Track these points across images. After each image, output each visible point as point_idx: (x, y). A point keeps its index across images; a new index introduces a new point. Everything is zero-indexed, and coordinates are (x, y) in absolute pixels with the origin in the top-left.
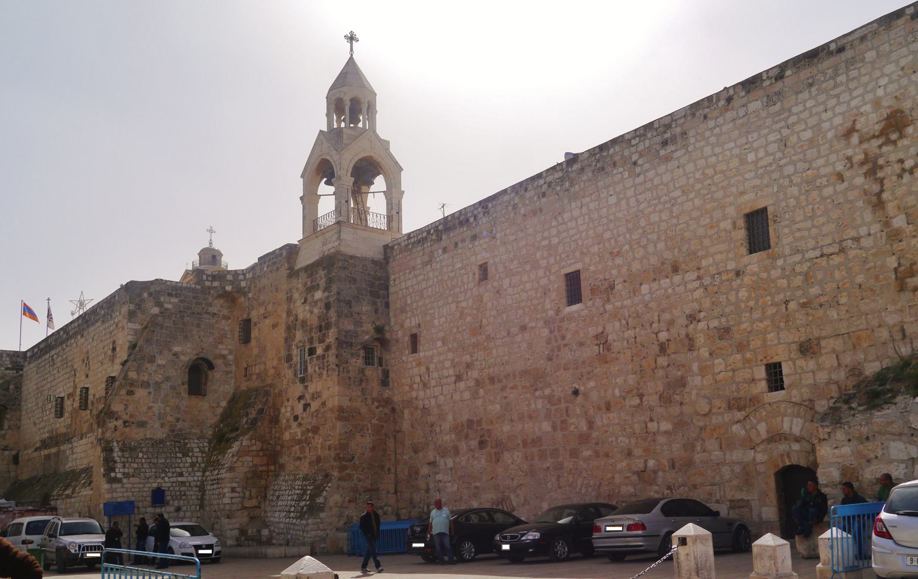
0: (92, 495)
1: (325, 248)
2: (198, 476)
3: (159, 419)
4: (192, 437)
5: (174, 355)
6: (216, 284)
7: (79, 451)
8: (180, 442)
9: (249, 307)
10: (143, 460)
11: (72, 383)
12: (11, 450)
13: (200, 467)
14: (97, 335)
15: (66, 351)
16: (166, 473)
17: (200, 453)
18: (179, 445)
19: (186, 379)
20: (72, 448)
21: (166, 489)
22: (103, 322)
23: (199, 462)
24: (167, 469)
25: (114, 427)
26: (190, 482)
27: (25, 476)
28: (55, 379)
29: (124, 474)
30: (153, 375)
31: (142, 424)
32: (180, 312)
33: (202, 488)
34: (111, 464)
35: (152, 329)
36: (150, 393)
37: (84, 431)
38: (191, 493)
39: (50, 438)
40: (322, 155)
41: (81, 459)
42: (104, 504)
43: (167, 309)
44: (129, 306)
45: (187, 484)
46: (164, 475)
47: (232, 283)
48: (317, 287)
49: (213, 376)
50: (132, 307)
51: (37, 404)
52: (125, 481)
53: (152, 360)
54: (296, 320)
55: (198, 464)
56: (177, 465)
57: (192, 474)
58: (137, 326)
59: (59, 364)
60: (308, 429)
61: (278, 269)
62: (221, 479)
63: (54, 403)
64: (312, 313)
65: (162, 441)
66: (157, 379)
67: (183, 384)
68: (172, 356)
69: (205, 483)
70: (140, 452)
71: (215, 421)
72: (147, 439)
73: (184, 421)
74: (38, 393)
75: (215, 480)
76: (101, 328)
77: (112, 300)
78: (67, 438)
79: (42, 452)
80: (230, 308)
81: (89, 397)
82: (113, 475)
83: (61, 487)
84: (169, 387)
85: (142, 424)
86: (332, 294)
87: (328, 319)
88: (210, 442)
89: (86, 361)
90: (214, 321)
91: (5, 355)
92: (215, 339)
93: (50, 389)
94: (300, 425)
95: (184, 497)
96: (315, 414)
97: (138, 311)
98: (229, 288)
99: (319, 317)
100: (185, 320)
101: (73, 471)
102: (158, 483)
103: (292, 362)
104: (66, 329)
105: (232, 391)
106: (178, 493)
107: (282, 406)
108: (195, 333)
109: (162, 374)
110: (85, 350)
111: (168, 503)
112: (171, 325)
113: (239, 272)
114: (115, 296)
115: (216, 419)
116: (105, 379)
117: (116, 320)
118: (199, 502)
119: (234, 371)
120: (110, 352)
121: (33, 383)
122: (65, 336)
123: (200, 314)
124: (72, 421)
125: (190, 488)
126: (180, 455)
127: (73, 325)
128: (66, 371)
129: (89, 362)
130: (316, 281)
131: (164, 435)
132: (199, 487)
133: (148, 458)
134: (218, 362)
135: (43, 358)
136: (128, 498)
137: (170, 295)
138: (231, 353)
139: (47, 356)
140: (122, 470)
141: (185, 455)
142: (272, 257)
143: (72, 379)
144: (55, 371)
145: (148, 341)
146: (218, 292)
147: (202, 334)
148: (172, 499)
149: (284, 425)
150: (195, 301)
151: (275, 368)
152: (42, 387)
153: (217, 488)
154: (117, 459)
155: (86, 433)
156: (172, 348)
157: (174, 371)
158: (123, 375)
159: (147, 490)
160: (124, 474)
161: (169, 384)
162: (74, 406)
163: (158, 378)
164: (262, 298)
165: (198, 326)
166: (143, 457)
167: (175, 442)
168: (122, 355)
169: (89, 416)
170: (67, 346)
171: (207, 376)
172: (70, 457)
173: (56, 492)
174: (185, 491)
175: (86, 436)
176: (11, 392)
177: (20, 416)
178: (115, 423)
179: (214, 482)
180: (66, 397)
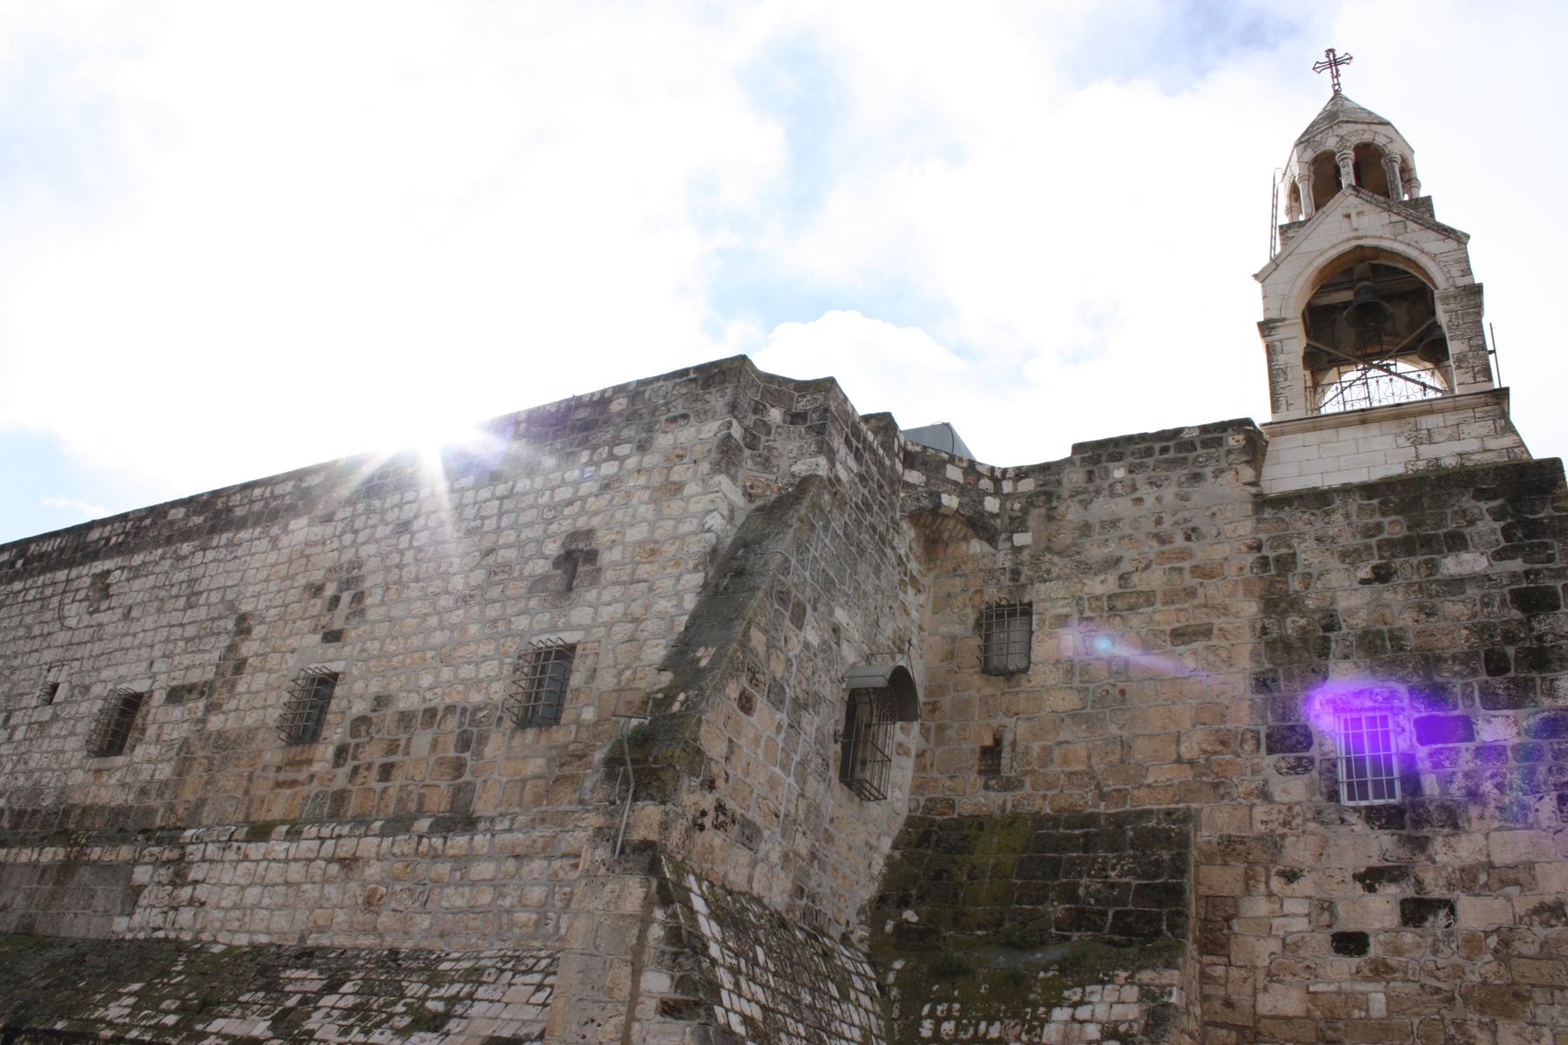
1: (1428, 452)
6: (914, 477)
9: (1015, 574)
19: (841, 729)
40: (1358, 238)
43: (838, 479)
47: (960, 489)
48: (1457, 542)
54: (1329, 628)
60: (1437, 991)
61: (1197, 478)
64: (1428, 615)
86: (1551, 565)
87: (1540, 638)
94: (1380, 971)
96: (1493, 941)
97: (747, 452)
98: (950, 501)
99: (1482, 630)
103: (1314, 752)
105: (905, 813)
107: (1248, 891)
113: (979, 468)
129: (359, 597)
130: (1438, 525)
142: (1157, 446)
149: (1263, 961)
151: (1191, 763)
164: (1095, 552)
180: (159, 697)
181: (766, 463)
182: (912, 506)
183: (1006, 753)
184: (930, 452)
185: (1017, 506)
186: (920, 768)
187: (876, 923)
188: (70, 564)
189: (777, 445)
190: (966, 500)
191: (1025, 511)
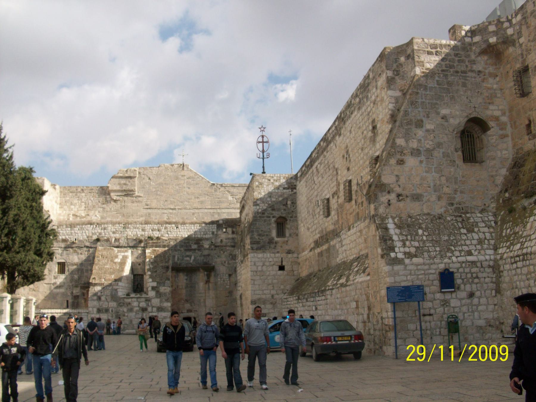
0: (369, 280)
2: (490, 255)
3: (435, 191)
4: (473, 211)
5: (442, 118)
6: (477, 39)
7: (348, 242)
8: (461, 216)
9: (522, 54)
10: (425, 238)
11: (336, 182)
12: (293, 253)
13: (489, 244)
14: (355, 125)
15: (327, 156)
16: (452, 252)
17: (487, 228)
18: (460, 219)
19: (459, 145)
20: (341, 241)
21: (455, 270)
22: (359, 109)
23: (488, 238)
24: (453, 248)
25: (387, 201)
26: (481, 262)
27: (304, 273)
28: (320, 185)
29: (405, 253)
30: (423, 141)
31: (417, 198)
32: (443, 71)
33: (496, 268)
34: (389, 242)
35: (415, 90)
36: (421, 162)
37: (351, 221)
38: (484, 275)
39: (321, 237)
41: (350, 249)
42: (388, 288)
44: (387, 73)
45: (479, 264)
46: (450, 255)
47: (495, 33)
49: (488, 141)
50: (390, 73)
51: (308, 212)
52: (407, 261)
53: (420, 124)
55: (486, 241)
56: (463, 242)
57: (482, 252)
58: (398, 94)
59: (322, 171)
62: (531, 253)
63: (321, 207)
65: (440, 217)
66: (428, 146)
67: (456, 151)
68: (440, 120)
69: (501, 262)
70: (420, 228)
71: (496, 192)
72: (425, 215)
73: (462, 192)
74: (308, 203)
75: (518, 256)
76: (359, 115)
77: (367, 82)
78: (335, 233)
79: (316, 251)
80: (496, 65)
81: (353, 188)
82: (393, 255)
83: (335, 278)
84: (441, 155)
85: (417, 198)
88: (495, 215)
89: (347, 156)
90: (480, 79)
91: (282, 178)
92: (484, 99)
93: (317, 196)
95: (476, 280)
97: (397, 77)
98: (493, 40)
100: (449, 79)
101: (344, 263)
102: (445, 264)
104: (325, 138)
105: (511, 157)
106: (469, 276)
108: (462, 93)
109: (432, 141)
110: (343, 146)
111: (458, 288)
112: (436, 86)
114: (369, 76)
115: (498, 189)
116: (368, 163)
117: (373, 98)
118: (495, 285)
119: (510, 135)
120: (370, 134)
121: (304, 196)
122: (325, 144)
123: (464, 72)
124: (338, 217)
125: (482, 269)
126: (464, 231)
127: (331, 131)
128: (328, 174)
129: (349, 156)
131: (442, 210)
132: (493, 267)
133: (429, 235)
134: (491, 124)
135: (310, 172)
136: (413, 282)
137: (429, 53)
138: (504, 114)
139: (311, 170)
140: (402, 249)
141: (470, 231)
143: (335, 179)
144: (320, 178)
145: (413, 103)
146: (480, 46)
147: (469, 93)
148: (463, 283)
150: (457, 59)
152: (311, 196)
153: (524, 266)
154: (395, 238)
155: (353, 224)
156: (439, 110)
157: (445, 136)
158: (390, 144)
159: (433, 271)
160: (405, 253)
161: (442, 151)
162: (339, 203)
163: (428, 144)
165: (464, 85)
166: (423, 235)
167: (456, 216)
168: (384, 128)
169: (354, 207)
170: (327, 152)
171: (482, 141)
172: (340, 250)
173: (330, 282)
174: (477, 273)
175: (353, 227)
176: (289, 206)
177: (297, 225)
178: (388, 197)
179: (517, 259)
180: (331, 197)
181: (403, 78)
182: (478, 50)
183: (532, 125)
184: (481, 26)
185: (518, 27)
186: (513, 139)
187: (498, 201)
188: (312, 166)
189: (406, 69)
190: (499, 36)
191: (521, 28)
